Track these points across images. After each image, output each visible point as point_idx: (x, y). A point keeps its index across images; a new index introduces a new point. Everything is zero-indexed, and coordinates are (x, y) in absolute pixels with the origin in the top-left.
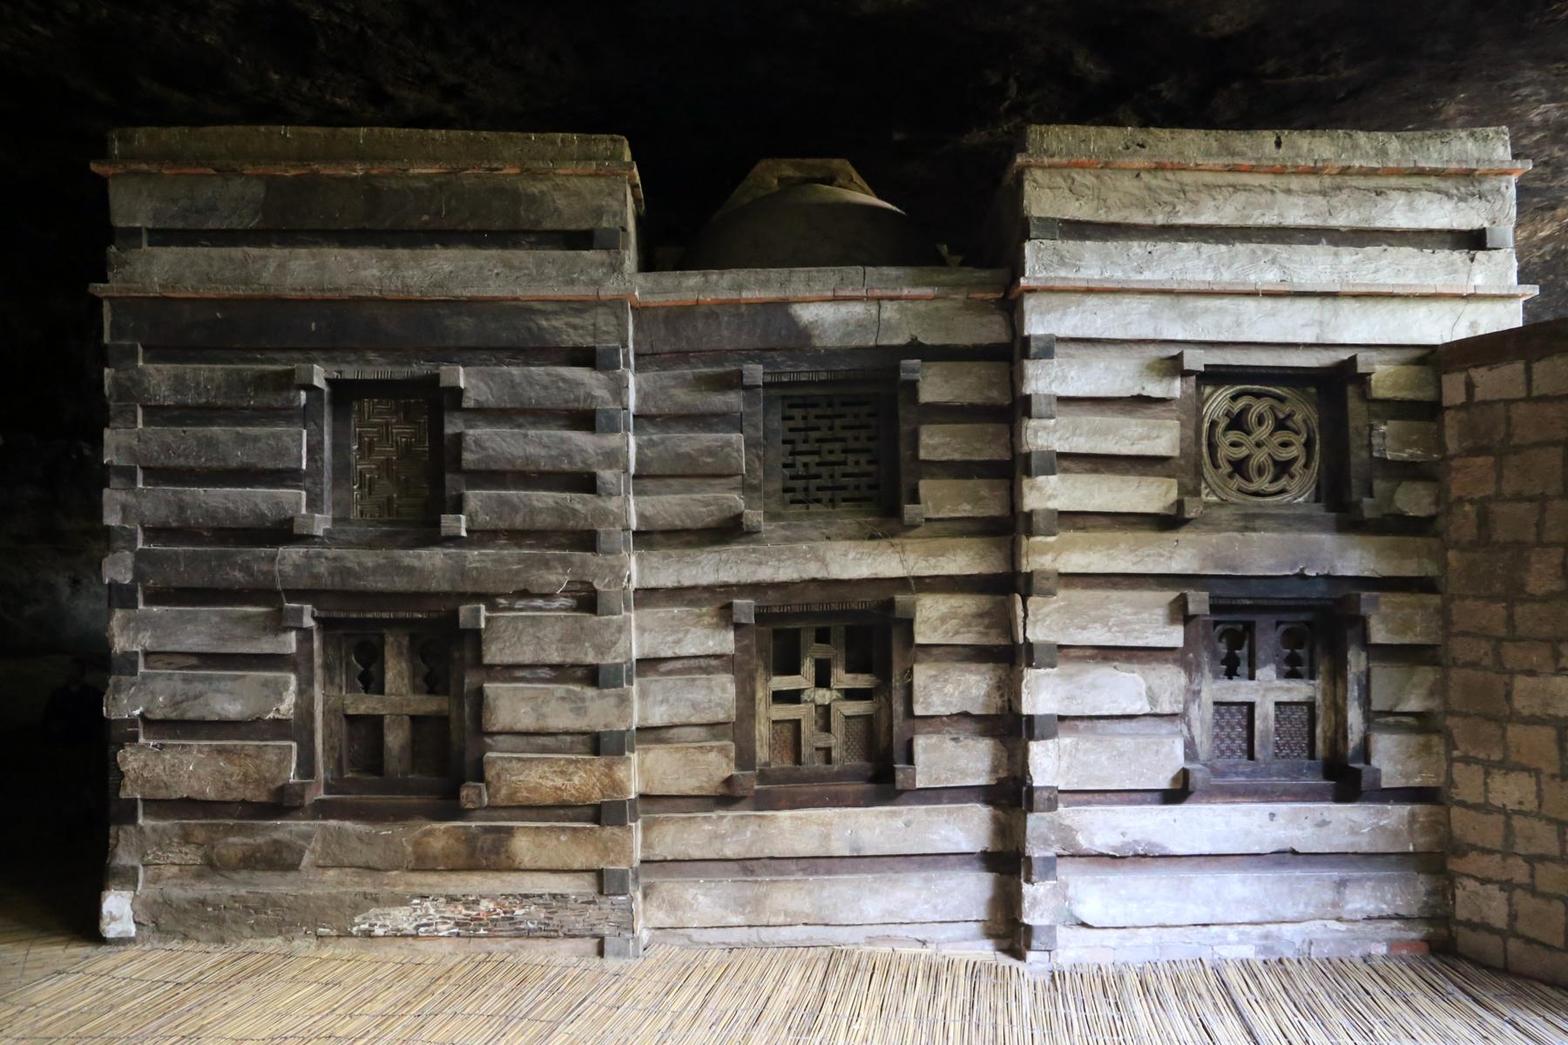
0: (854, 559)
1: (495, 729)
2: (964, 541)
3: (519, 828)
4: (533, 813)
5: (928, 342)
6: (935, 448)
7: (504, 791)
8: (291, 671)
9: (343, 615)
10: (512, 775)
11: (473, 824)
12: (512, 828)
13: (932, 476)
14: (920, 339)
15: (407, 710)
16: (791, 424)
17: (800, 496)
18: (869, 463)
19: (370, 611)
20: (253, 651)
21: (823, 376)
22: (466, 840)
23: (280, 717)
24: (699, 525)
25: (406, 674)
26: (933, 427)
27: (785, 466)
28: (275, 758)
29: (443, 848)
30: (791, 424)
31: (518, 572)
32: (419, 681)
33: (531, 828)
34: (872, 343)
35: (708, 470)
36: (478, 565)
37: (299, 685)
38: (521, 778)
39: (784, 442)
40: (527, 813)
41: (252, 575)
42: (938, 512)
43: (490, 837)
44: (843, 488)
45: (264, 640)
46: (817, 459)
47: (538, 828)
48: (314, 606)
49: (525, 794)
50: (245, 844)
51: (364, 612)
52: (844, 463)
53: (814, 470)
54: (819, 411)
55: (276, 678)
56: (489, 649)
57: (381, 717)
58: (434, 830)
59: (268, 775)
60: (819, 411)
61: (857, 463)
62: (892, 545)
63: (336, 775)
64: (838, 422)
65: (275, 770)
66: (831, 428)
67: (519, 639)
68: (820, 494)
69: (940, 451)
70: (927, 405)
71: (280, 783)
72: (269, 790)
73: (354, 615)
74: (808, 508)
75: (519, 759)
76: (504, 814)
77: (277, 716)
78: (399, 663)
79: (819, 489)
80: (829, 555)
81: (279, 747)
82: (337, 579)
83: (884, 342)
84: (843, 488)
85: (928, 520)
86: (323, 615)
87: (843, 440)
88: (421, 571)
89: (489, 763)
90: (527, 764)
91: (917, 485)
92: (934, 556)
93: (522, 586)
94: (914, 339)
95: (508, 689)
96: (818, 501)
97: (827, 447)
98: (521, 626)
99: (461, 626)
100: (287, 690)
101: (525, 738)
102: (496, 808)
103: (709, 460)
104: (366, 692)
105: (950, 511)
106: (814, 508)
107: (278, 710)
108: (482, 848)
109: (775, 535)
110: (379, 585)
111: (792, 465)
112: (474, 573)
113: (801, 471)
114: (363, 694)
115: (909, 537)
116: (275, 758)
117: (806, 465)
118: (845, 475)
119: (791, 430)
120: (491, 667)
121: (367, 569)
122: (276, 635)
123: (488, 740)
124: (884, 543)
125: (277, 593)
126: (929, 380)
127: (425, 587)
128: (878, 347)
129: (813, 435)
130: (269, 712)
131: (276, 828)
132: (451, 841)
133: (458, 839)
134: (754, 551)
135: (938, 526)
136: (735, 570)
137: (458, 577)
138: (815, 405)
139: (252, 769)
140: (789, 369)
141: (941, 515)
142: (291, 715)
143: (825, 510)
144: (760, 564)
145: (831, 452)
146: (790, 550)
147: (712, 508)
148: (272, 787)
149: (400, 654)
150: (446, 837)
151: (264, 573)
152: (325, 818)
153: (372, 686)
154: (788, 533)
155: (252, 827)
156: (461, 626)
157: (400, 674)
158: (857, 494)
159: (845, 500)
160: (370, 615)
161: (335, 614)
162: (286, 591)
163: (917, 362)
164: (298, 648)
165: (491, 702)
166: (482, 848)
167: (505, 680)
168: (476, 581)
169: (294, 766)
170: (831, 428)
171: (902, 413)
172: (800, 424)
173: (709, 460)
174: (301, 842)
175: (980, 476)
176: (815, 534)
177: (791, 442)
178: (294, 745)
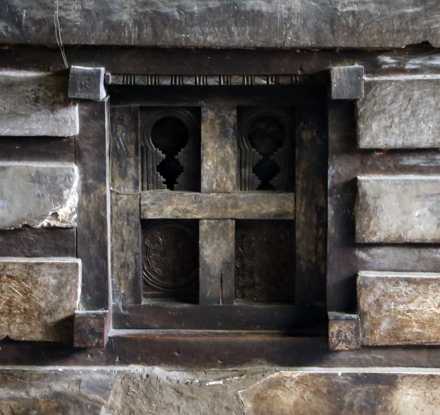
1: (374, 239)
3: (404, 376)
4: (423, 356)
7: (385, 325)
8: (70, 160)
9: (150, 81)
10: (397, 303)
11: (340, 371)
12: (395, 376)
15: (232, 213)
19: (189, 76)
20: (17, 133)
22: (329, 392)
23: (58, 224)
25: (233, 162)
28: (53, 281)
29: (296, 404)
31: (414, 18)
32: (248, 172)
33: (420, 377)
36: (355, 8)
37: (84, 179)
38: (412, 307)
40: (413, 355)
41: (19, 25)
43: (362, 390)
45: (34, 117)
47: (432, 376)
48: (107, 70)
49: (416, 329)
50: (13, 398)
51: (182, 76)
55: (53, 169)
56: (368, 127)
57: (195, 223)
58: (284, 379)
59: (43, 304)
63: (129, 302)
65: (53, 298)
67: (413, 113)
71: (61, 315)
72: (45, 326)
73: (166, 82)
75: (409, 281)
76: (380, 355)
77: (53, 223)
78: (222, 147)
81: (59, 266)
82: (147, 31)
86: (120, 81)
88: (272, 17)
89: (366, 286)
90: (421, 288)
93: (420, 38)
95: (395, 183)
98: (416, 94)
99: (334, 96)
100: (69, 187)
101: (416, 251)
102: (366, 348)
104: (171, 187)
107: (55, 215)
108: (351, 405)
110: (209, 39)
112: (350, 19)
114: (167, 191)
116: (53, 281)
120: (369, 152)
121: (192, 14)
122: (53, 110)
123: (362, 254)
125: (56, 49)
127: (276, 41)
130: (42, 218)
131: (57, 376)
132: (308, 395)
133: (317, 392)
137: (326, 28)
139: (18, 298)
142: (73, 222)
148: (49, 320)
149: (224, 134)
150: (299, 390)
151: (39, 23)
152: (125, 361)
153: (180, 179)
155: (23, 376)
156: (334, 96)
157: (224, 162)
160: (189, 82)
161: (139, 81)
162: (67, 47)
164: (82, 129)
165: (370, 201)
166: (351, 405)
167: (388, 171)
168: (352, 31)
169: (79, 291)
174: (94, 396)
178: (79, 262)
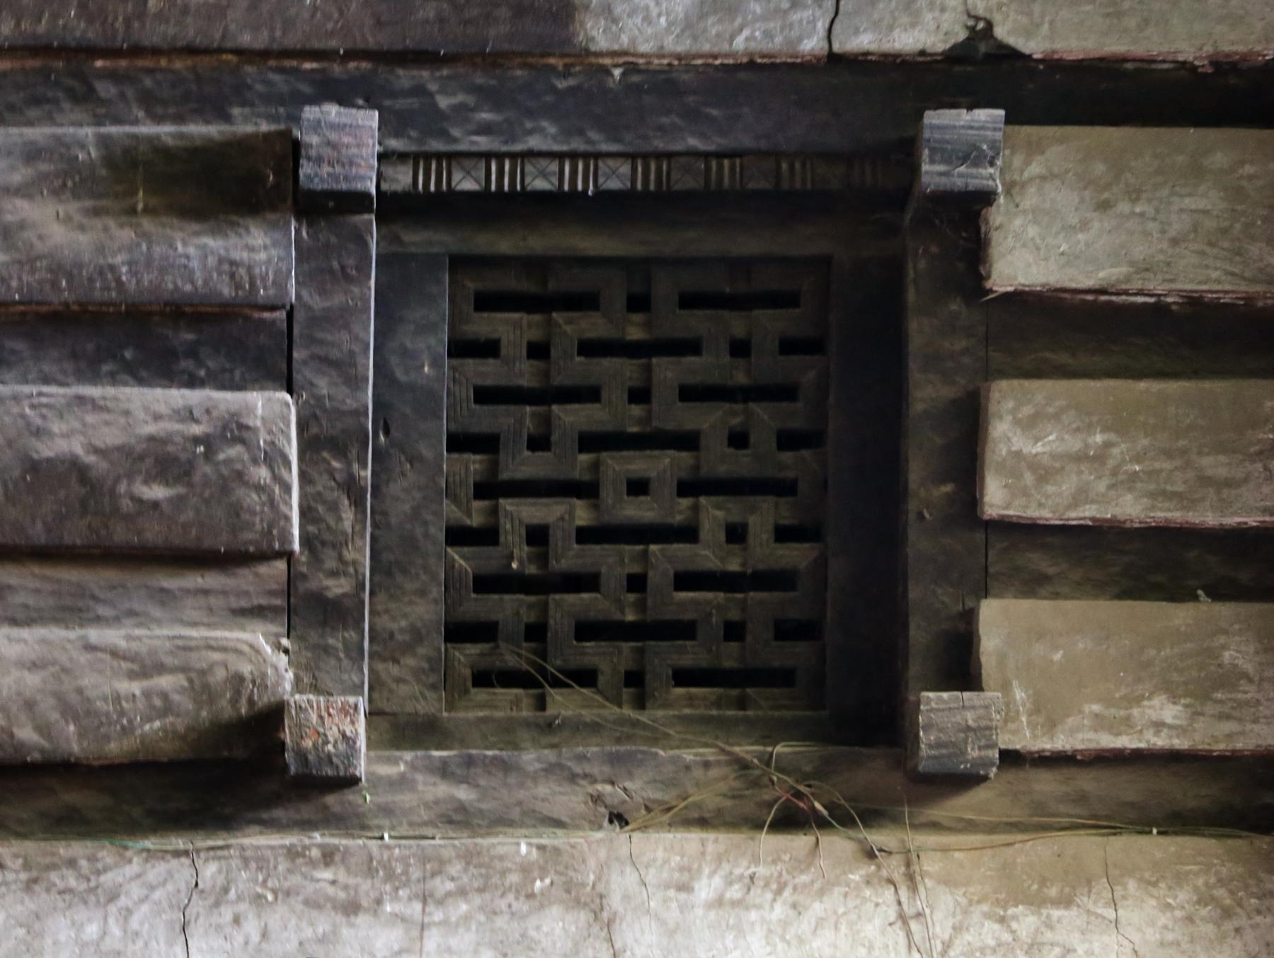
0: (719, 902)
2: (1156, 846)
5: (1034, 46)
6: (1045, 473)
13: (1032, 585)
14: (1000, 32)
16: (487, 372)
17: (513, 657)
18: (783, 534)
21: (616, 177)
24: (115, 748)
26: (1042, 391)
27: (457, 536)
30: (487, 372)
34: (812, 45)
35: (153, 533)
39: (458, 443)
42: (1052, 726)
44: (682, 630)
46: (582, 514)
52: (688, 533)
53: (569, 557)
54: (593, 326)
60: (593, 326)
61: (736, 534)
62: (870, 855)
64: (668, 371)
66: (640, 395)
68: (593, 653)
69: (1067, 486)
70: (1020, 300)
74: (541, 704)
79: (587, 630)
80: (621, 883)
83: (862, 40)
84: (682, 630)
85: (1011, 759)
87: (687, 441)
91: (970, 617)
92: (1037, 902)
94: (981, 32)
96: (586, 678)
97: (620, 465)
103: (158, 492)
105: (1100, 723)
106: (563, 703)
109: (405, 799)
111: (487, 536)
113: (520, 560)
115: (935, 826)
117: (537, 536)
118: (686, 580)
119: (485, 395)
124: (837, 844)
126: (1030, 199)
128: (835, 60)
129: (571, 417)
134: (328, 857)
135: (1045, 783)
136: (252, 927)
138: (583, 302)
140: (483, 143)
141: (1060, 742)
143: (612, 711)
144: (351, 908)
145: (638, 487)
146: (468, 858)
147: (165, 682)
154: (463, 794)
158: (730, 654)
159: (683, 677)
163: (987, 117)
170: (640, 395)
171: (919, 332)
172: (524, 374)
173: (158, 492)
175: (1219, 592)
176: (568, 800)
177: (486, 444)
